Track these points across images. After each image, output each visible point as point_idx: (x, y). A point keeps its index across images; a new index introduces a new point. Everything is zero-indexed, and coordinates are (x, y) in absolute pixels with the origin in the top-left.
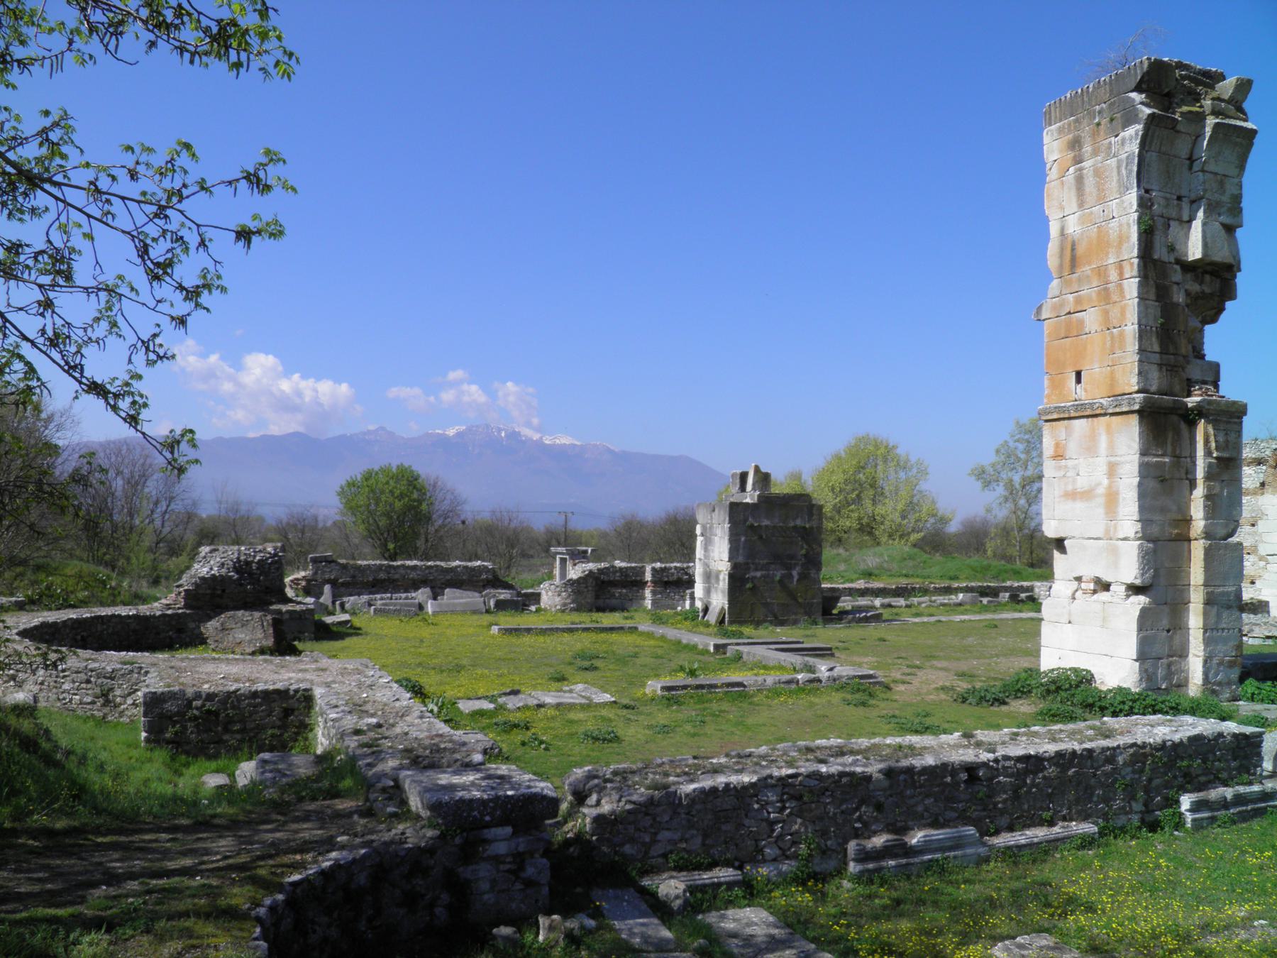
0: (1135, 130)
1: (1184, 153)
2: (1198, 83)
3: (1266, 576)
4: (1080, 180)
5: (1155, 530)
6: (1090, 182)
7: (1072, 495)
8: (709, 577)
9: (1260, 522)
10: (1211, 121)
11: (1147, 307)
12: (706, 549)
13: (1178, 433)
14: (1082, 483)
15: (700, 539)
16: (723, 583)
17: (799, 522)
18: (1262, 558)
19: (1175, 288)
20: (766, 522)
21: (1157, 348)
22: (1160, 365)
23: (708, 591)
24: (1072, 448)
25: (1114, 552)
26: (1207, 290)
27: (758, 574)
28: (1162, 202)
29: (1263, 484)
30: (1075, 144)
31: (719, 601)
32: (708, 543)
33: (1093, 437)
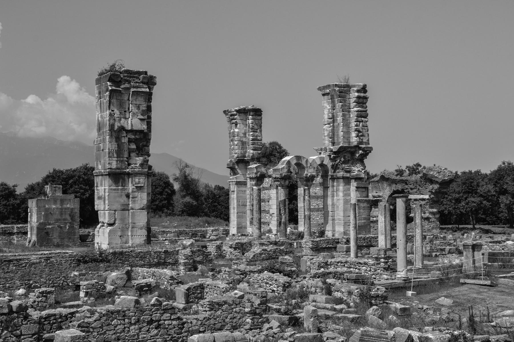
0: (108, 93)
1: (126, 98)
2: (131, 77)
3: (272, 222)
4: (101, 103)
5: (114, 207)
6: (102, 105)
7: (99, 198)
8: (32, 228)
9: (270, 201)
10: (132, 90)
11: (112, 145)
12: (31, 218)
13: (124, 180)
14: (100, 194)
15: (29, 214)
16: (35, 232)
17: (68, 206)
18: (271, 215)
19: (123, 138)
20: (54, 206)
21: (115, 156)
22: (117, 161)
23: (31, 234)
24: (99, 185)
25: (105, 214)
26: (137, 137)
27: (50, 227)
28: (118, 113)
29: (271, 185)
30: (100, 93)
31: (34, 238)
32: (31, 215)
33: (102, 181)
